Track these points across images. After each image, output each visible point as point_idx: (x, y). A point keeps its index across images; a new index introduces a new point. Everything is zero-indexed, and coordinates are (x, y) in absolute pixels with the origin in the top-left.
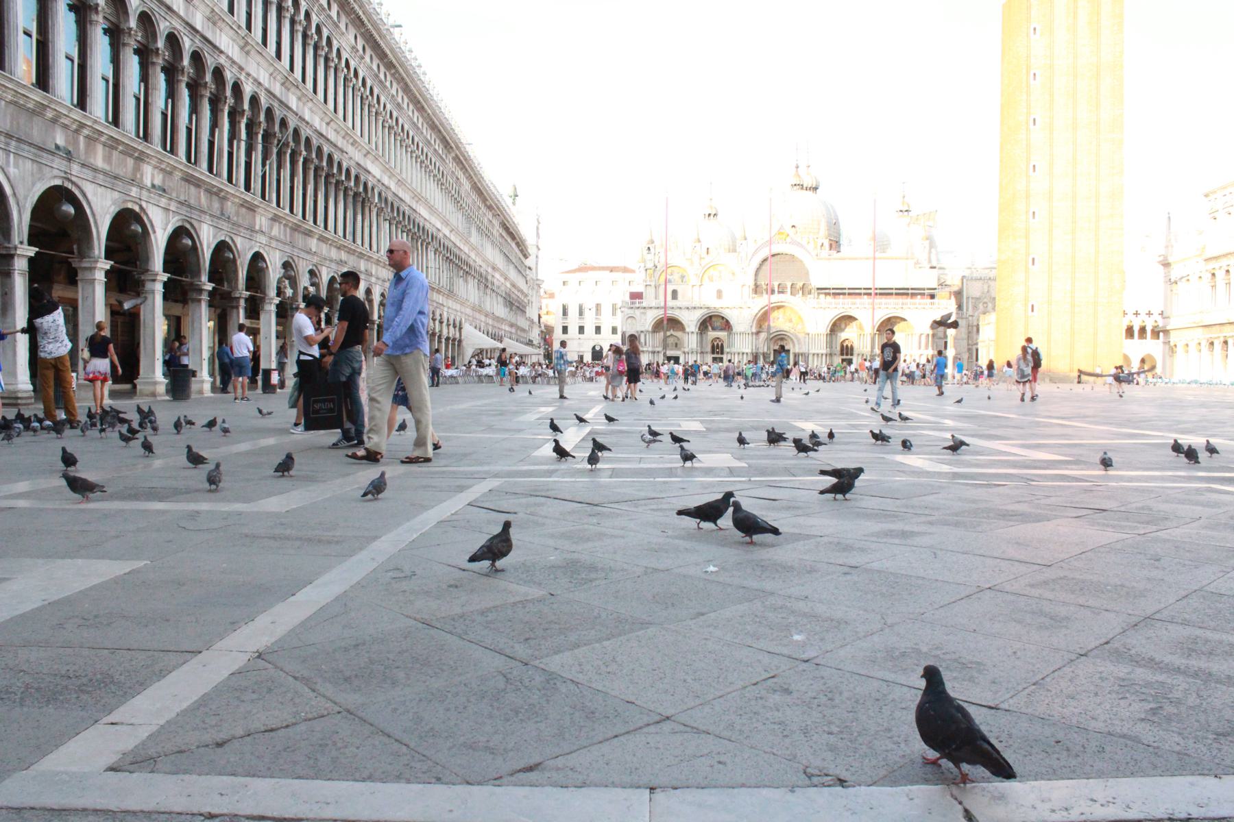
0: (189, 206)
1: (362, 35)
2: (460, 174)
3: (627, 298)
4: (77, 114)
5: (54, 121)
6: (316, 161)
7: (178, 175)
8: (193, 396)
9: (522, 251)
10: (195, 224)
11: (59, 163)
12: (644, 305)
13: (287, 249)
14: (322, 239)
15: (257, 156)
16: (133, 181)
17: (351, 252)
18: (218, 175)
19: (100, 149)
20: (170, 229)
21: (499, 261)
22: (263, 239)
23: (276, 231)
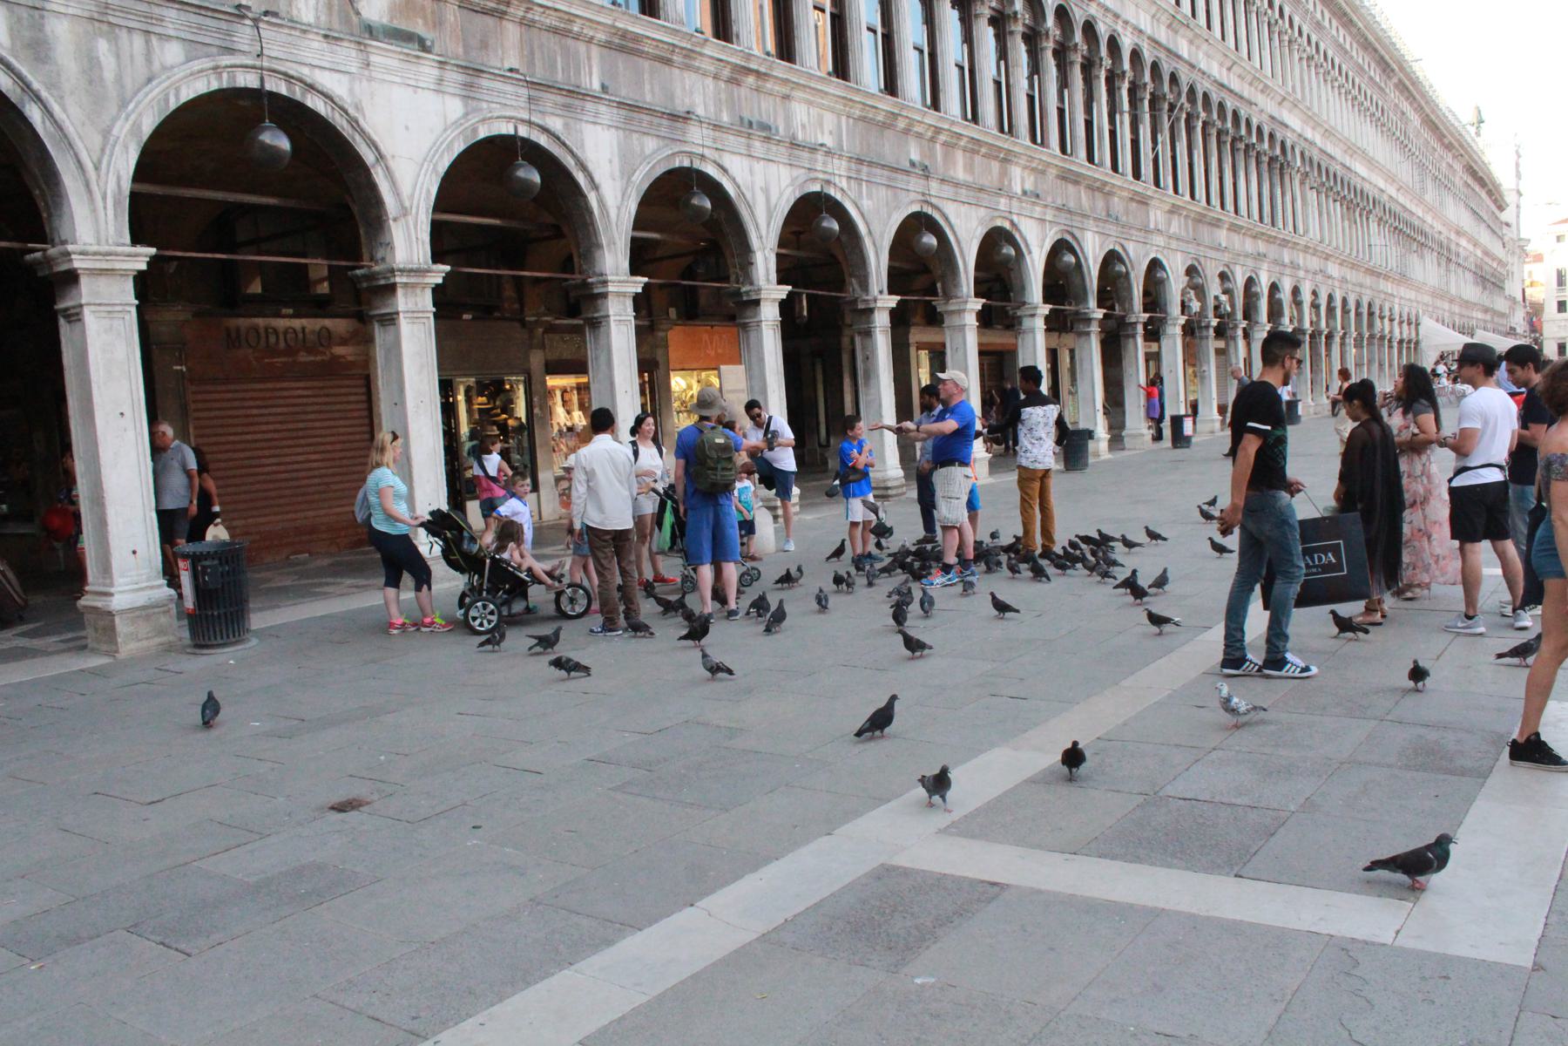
0: (1070, 212)
2: (1405, 106)
4: (931, 118)
5: (907, 131)
6: (1219, 123)
7: (1053, 172)
8: (1091, 460)
9: (1495, 202)
10: (1076, 232)
11: (916, 184)
13: (1192, 249)
14: (1234, 228)
16: (1000, 191)
17: (1270, 240)
18: (1101, 164)
19: (959, 156)
21: (1465, 220)
22: (1159, 240)
23: (1176, 226)
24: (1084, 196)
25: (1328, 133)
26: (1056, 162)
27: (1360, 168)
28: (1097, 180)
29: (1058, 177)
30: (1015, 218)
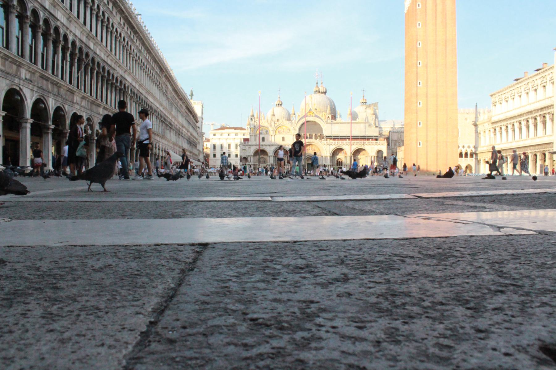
0: (43, 89)
1: (123, 17)
2: (167, 83)
3: (242, 141)
6: (102, 73)
7: (37, 75)
9: (195, 119)
12: (250, 144)
13: (89, 112)
15: (75, 69)
18: (57, 76)
20: (34, 99)
21: (185, 123)
23: (84, 103)
24: (50, 86)
25: (140, 85)
26: (39, 71)
27: (151, 99)
28: (55, 81)
29: (40, 76)
30: (21, 87)
